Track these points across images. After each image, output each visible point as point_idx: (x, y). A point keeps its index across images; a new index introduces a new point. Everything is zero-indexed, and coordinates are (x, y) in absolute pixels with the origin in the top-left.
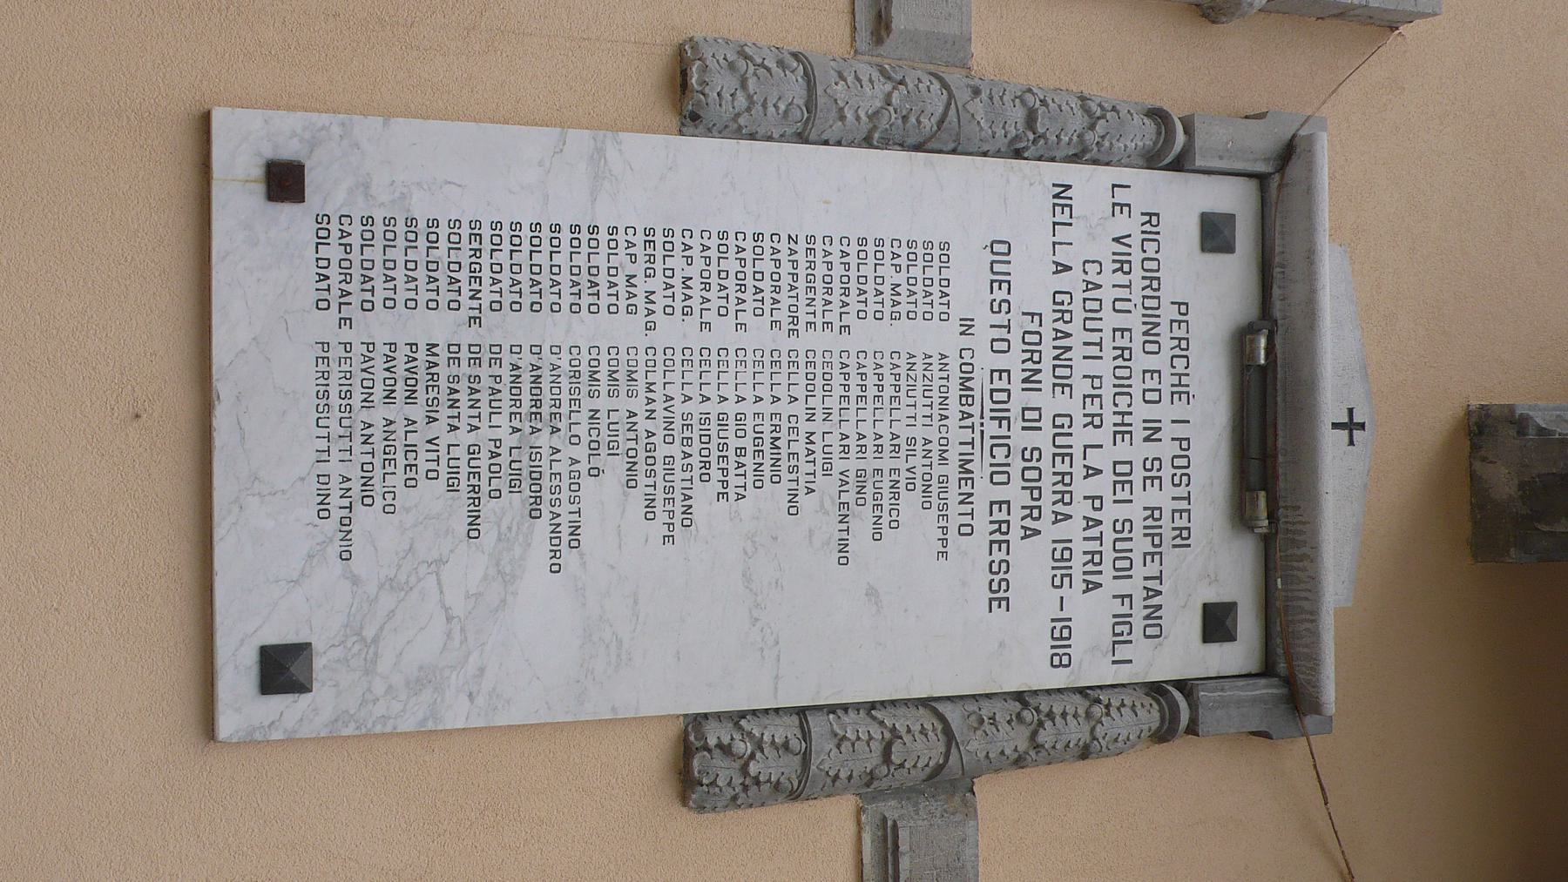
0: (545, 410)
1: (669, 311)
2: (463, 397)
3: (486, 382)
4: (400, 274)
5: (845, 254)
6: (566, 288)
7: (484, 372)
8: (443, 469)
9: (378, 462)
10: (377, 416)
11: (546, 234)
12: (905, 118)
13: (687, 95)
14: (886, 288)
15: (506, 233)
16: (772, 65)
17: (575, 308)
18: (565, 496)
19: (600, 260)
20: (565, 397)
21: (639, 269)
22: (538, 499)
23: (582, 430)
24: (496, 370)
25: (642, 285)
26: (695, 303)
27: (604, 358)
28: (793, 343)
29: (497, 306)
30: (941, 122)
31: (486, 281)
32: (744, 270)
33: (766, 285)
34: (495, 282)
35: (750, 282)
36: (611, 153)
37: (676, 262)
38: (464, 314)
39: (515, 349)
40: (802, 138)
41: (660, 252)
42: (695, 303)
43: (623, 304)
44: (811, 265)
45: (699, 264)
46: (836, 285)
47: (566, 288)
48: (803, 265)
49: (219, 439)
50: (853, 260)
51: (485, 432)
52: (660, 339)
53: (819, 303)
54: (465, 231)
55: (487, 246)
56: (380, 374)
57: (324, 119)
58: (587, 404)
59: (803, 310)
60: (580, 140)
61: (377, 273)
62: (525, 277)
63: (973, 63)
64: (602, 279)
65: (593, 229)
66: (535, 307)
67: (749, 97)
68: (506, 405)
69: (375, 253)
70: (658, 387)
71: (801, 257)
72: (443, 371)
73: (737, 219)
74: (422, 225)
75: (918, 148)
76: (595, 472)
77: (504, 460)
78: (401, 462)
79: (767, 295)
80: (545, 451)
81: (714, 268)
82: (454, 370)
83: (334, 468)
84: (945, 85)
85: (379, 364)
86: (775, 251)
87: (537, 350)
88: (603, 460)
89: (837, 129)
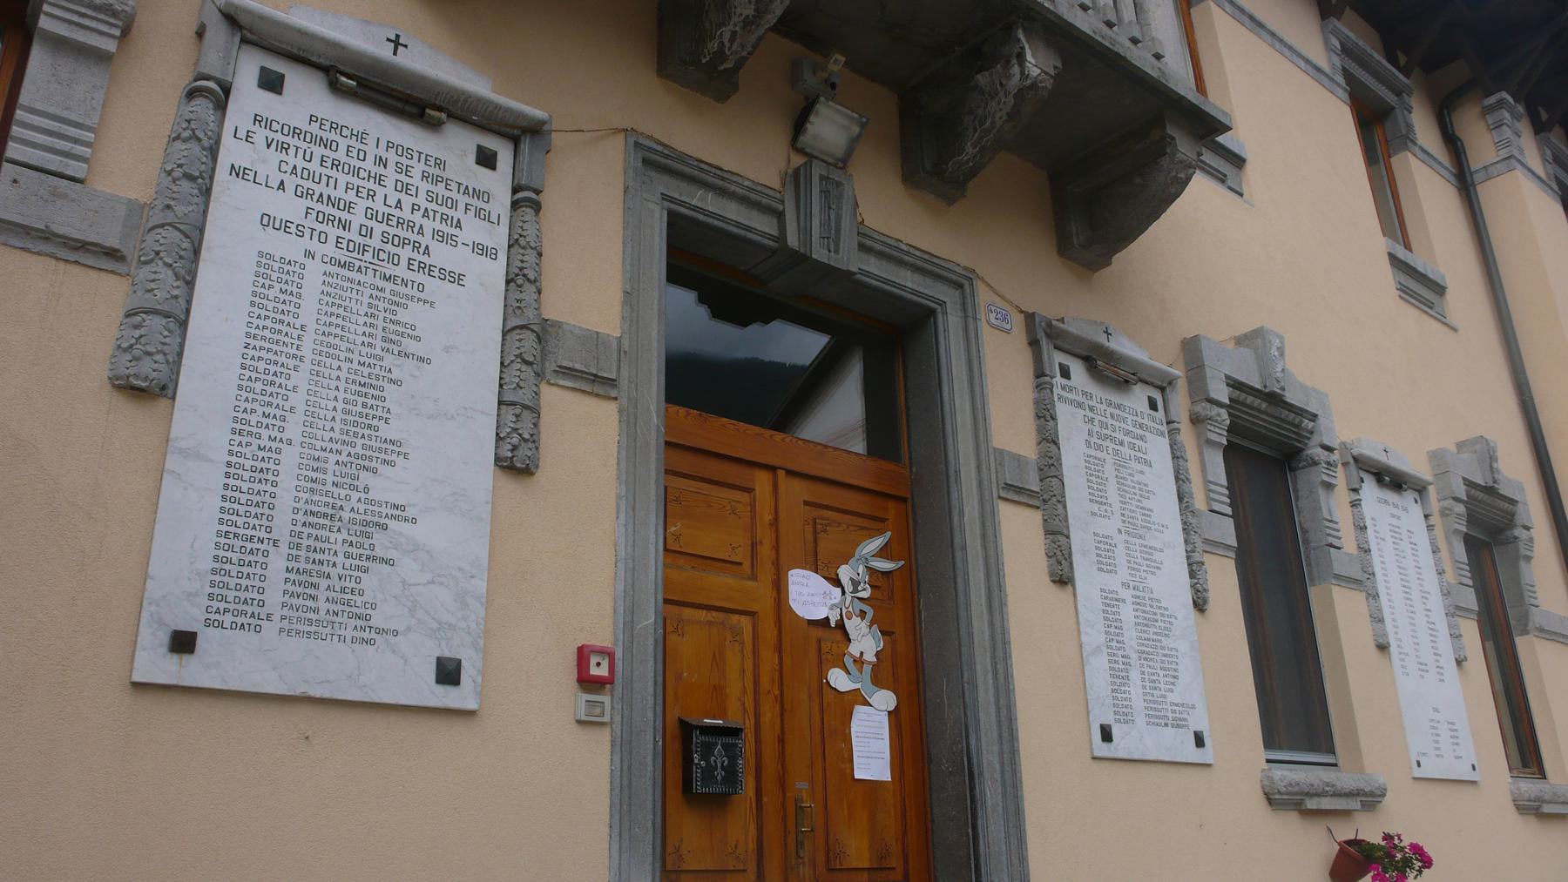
0: (330, 511)
1: (282, 430)
2: (318, 556)
3: (311, 542)
4: (244, 582)
5: (259, 317)
6: (262, 487)
7: (305, 542)
8: (356, 574)
9: (348, 609)
10: (323, 606)
11: (229, 493)
12: (181, 257)
13: (148, 389)
14: (282, 297)
15: (226, 517)
16: (137, 333)
17: (275, 484)
18: (377, 509)
19: (248, 464)
20: (324, 499)
21: (255, 442)
22: (377, 524)
23: (343, 493)
24: (305, 536)
25: (265, 442)
26: (279, 413)
27: (304, 472)
28: (307, 360)
29: (269, 530)
30: (187, 236)
31: (253, 533)
32: (262, 378)
33: (273, 368)
34: (254, 528)
35: (270, 378)
36: (183, 444)
37: (254, 419)
38: (271, 549)
39: (294, 522)
40: (184, 324)
41: (246, 428)
42: (279, 413)
43: (274, 456)
44: (263, 338)
45: (255, 406)
46: (277, 326)
47: (262, 487)
48: (262, 344)
49: (327, 695)
50: (263, 313)
51: (337, 547)
52: (297, 439)
53: (286, 339)
54: (223, 541)
55: (233, 529)
56: (300, 602)
57: (145, 615)
58: (329, 487)
59: (288, 350)
60: (172, 462)
61: (243, 595)
62: (254, 510)
63: (143, 200)
64: (259, 465)
65: (229, 464)
66: (271, 507)
67: (158, 352)
68: (325, 533)
69: (231, 595)
70: (324, 445)
71: (258, 344)
72: (302, 566)
73: (232, 377)
74: (216, 565)
75: (197, 252)
76: (367, 490)
77: (354, 539)
78: (349, 596)
79: (279, 369)
80: (352, 515)
81: (260, 397)
82: (302, 559)
83: (349, 633)
84: (162, 226)
85: (295, 601)
86: (253, 358)
87: (296, 511)
88: (360, 484)
89: (182, 302)
